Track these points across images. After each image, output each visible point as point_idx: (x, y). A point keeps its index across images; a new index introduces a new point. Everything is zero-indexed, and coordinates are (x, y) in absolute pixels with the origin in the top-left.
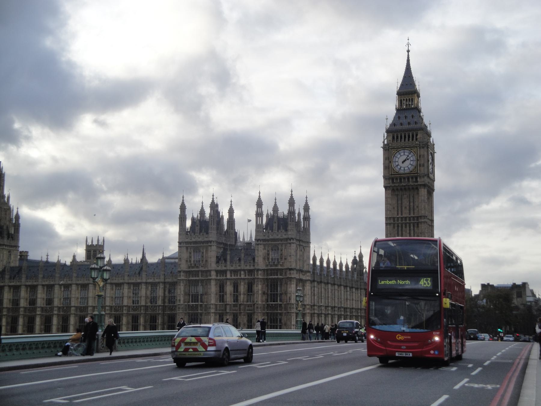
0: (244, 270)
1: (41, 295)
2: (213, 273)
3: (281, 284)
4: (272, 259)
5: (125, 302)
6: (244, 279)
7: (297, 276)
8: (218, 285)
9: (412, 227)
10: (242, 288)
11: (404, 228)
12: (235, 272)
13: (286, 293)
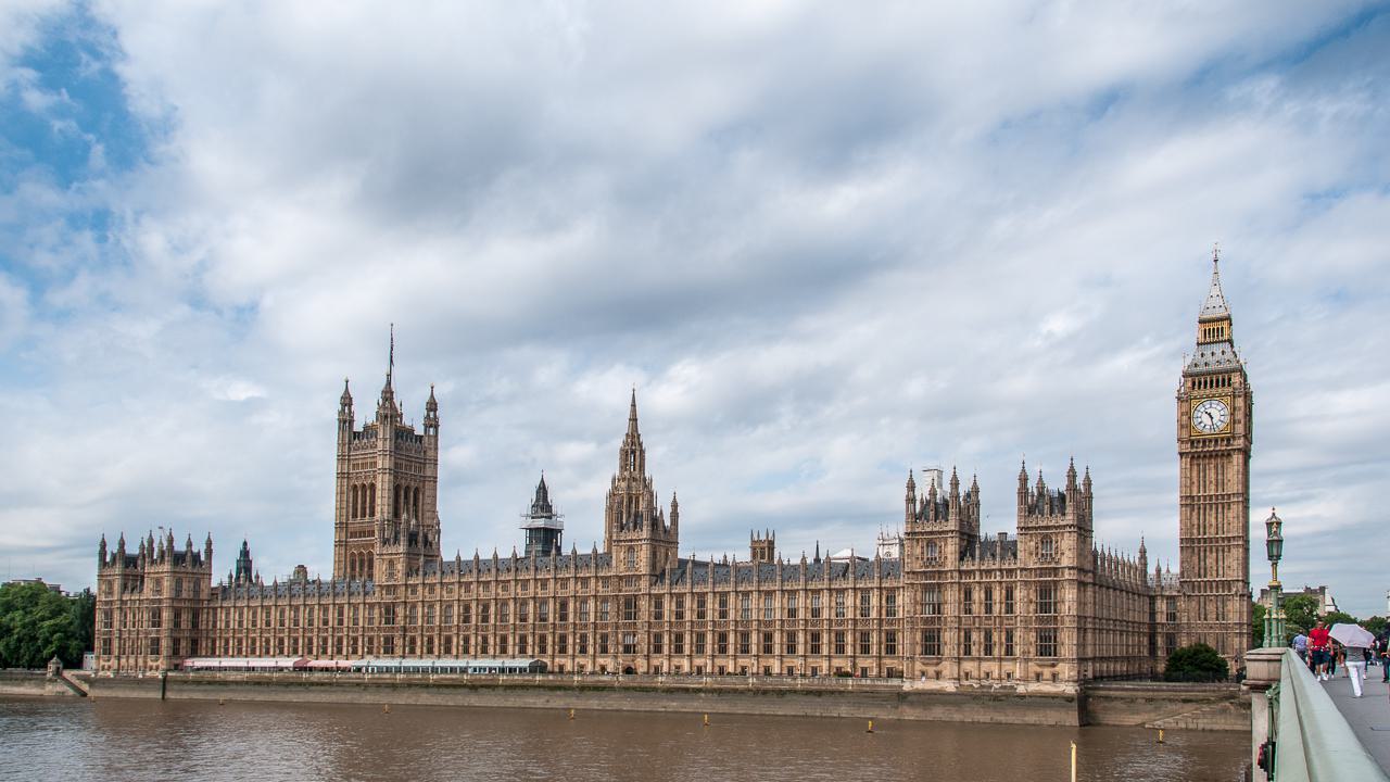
0: (1001, 570)
1: (711, 605)
2: (956, 574)
3: (1055, 590)
4: (1043, 555)
5: (825, 615)
6: (1001, 583)
8: (962, 592)
9: (1220, 510)
11: (1207, 511)
12: (989, 572)
13: (1063, 602)
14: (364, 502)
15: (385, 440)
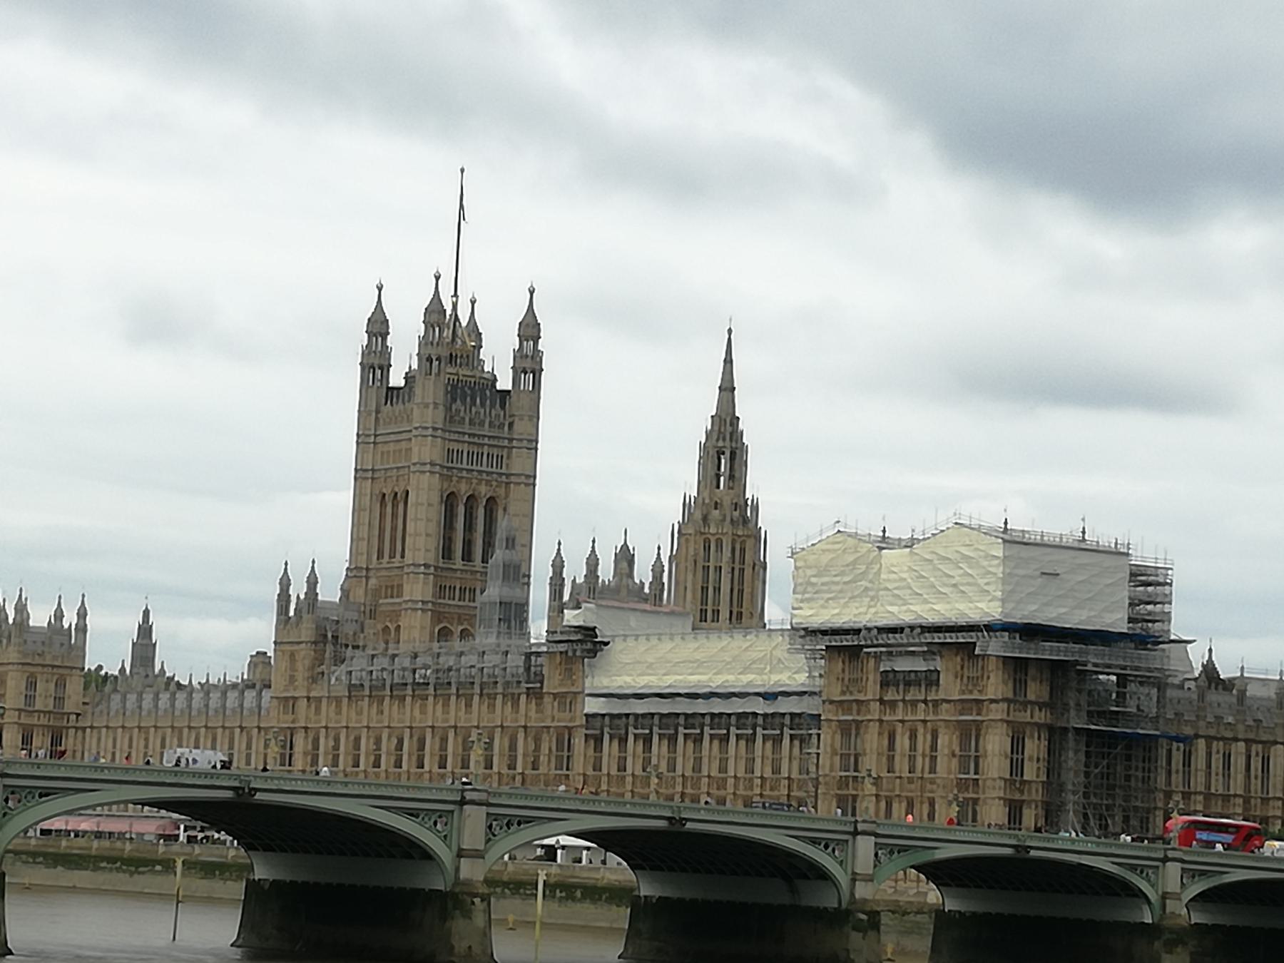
4: (968, 677)
6: (924, 722)
7: (1025, 717)
8: (886, 735)
10: (923, 742)
12: (914, 703)
14: (394, 529)
15: (427, 406)
